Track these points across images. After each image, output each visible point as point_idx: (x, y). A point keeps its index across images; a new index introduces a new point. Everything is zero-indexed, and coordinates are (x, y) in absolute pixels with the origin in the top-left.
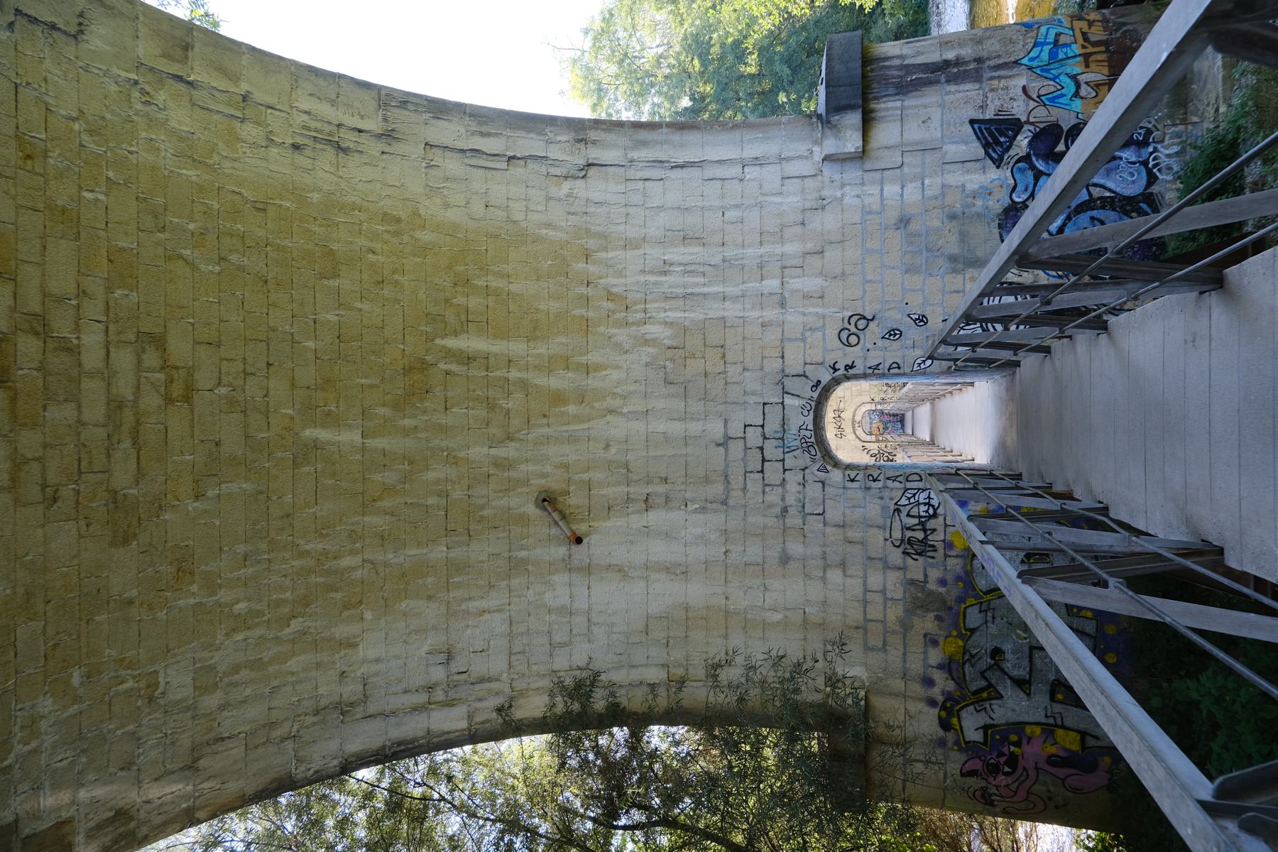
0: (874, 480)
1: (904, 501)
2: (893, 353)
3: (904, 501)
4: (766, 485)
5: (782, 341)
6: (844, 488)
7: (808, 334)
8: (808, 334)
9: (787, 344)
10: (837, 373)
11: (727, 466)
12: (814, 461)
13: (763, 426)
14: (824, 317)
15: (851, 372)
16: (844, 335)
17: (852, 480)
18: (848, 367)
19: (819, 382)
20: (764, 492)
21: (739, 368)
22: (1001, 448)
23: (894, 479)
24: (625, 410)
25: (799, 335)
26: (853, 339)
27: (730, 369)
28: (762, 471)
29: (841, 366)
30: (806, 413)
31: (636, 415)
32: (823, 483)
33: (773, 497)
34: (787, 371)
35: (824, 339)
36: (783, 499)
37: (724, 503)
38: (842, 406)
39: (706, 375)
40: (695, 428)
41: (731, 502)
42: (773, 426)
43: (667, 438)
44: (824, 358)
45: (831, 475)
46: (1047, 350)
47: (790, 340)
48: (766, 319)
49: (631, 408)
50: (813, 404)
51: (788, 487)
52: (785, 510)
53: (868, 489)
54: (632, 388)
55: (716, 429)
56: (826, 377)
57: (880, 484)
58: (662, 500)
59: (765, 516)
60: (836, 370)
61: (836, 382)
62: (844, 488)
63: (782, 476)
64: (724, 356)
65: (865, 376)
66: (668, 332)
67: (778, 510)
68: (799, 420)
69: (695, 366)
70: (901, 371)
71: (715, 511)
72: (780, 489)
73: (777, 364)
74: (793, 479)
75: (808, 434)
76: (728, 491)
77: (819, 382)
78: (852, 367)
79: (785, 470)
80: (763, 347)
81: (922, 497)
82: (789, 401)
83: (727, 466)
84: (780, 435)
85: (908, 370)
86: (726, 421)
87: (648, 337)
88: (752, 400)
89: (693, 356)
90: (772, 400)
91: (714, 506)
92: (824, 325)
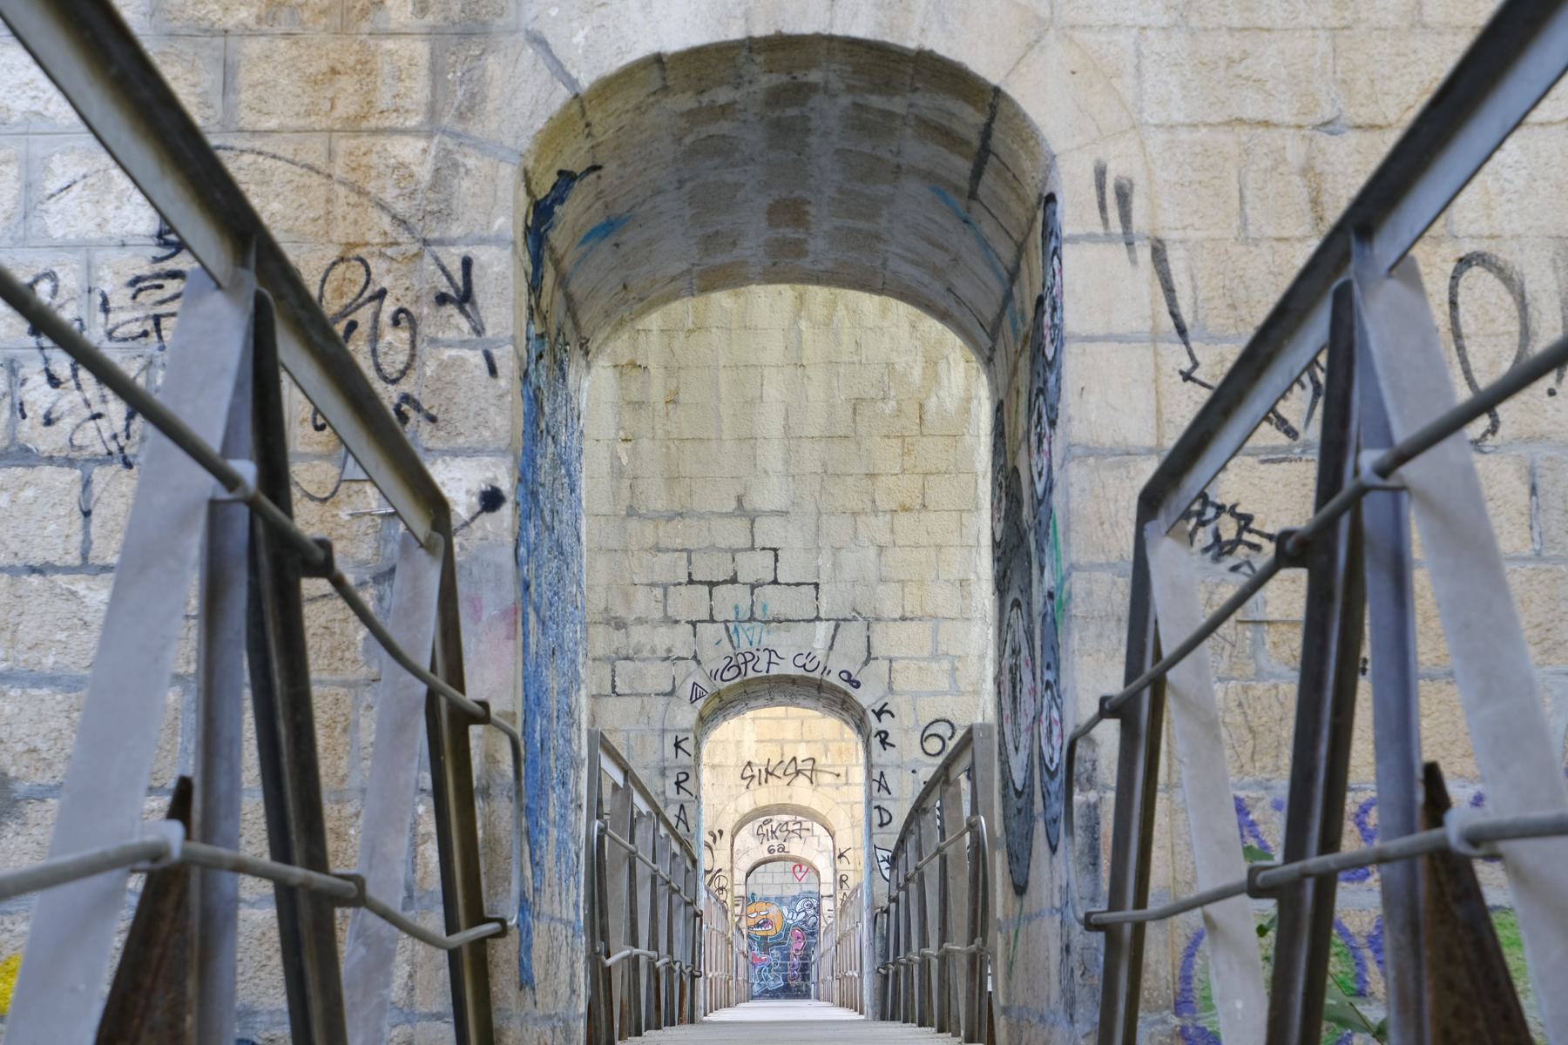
0: (678, 784)
4: (665, 588)
5: (934, 617)
6: (664, 731)
7: (946, 665)
8: (946, 665)
9: (927, 626)
10: (872, 717)
11: (701, 516)
12: (713, 676)
13: (775, 582)
14: (976, 693)
15: (875, 742)
16: (943, 729)
17: (677, 745)
18: (884, 738)
19: (858, 685)
20: (652, 585)
21: (884, 538)
24: (803, 325)
25: (943, 647)
27: (882, 521)
28: (691, 582)
29: (886, 723)
30: (800, 661)
31: (795, 345)
32: (671, 693)
33: (644, 603)
34: (877, 628)
35: (935, 694)
36: (640, 621)
37: (632, 512)
38: (826, 778)
39: (871, 476)
40: (772, 455)
41: (633, 525)
42: (775, 601)
43: (752, 403)
44: (903, 693)
45: (687, 707)
47: (936, 631)
48: (973, 588)
49: (807, 334)
50: (816, 675)
51: (663, 630)
52: (620, 624)
53: (663, 773)
54: (846, 339)
55: (768, 495)
56: (866, 697)
58: (635, 395)
59: (608, 588)
60: (879, 714)
61: (860, 725)
62: (664, 731)
63: (683, 618)
64: (906, 509)
65: (869, 767)
66: (951, 405)
67: (619, 611)
68: (787, 652)
69: (886, 456)
70: (876, 829)
71: (615, 495)
72: (658, 615)
73: (890, 609)
74: (679, 640)
75: (762, 666)
76: (654, 517)
77: (858, 685)
78: (883, 742)
79: (693, 624)
80: (921, 582)
82: (822, 631)
83: (701, 516)
84: (758, 614)
85: (877, 840)
86: (783, 513)
87: (942, 366)
88: (825, 562)
89: (906, 452)
90: (823, 599)
91: (626, 493)
92: (963, 694)
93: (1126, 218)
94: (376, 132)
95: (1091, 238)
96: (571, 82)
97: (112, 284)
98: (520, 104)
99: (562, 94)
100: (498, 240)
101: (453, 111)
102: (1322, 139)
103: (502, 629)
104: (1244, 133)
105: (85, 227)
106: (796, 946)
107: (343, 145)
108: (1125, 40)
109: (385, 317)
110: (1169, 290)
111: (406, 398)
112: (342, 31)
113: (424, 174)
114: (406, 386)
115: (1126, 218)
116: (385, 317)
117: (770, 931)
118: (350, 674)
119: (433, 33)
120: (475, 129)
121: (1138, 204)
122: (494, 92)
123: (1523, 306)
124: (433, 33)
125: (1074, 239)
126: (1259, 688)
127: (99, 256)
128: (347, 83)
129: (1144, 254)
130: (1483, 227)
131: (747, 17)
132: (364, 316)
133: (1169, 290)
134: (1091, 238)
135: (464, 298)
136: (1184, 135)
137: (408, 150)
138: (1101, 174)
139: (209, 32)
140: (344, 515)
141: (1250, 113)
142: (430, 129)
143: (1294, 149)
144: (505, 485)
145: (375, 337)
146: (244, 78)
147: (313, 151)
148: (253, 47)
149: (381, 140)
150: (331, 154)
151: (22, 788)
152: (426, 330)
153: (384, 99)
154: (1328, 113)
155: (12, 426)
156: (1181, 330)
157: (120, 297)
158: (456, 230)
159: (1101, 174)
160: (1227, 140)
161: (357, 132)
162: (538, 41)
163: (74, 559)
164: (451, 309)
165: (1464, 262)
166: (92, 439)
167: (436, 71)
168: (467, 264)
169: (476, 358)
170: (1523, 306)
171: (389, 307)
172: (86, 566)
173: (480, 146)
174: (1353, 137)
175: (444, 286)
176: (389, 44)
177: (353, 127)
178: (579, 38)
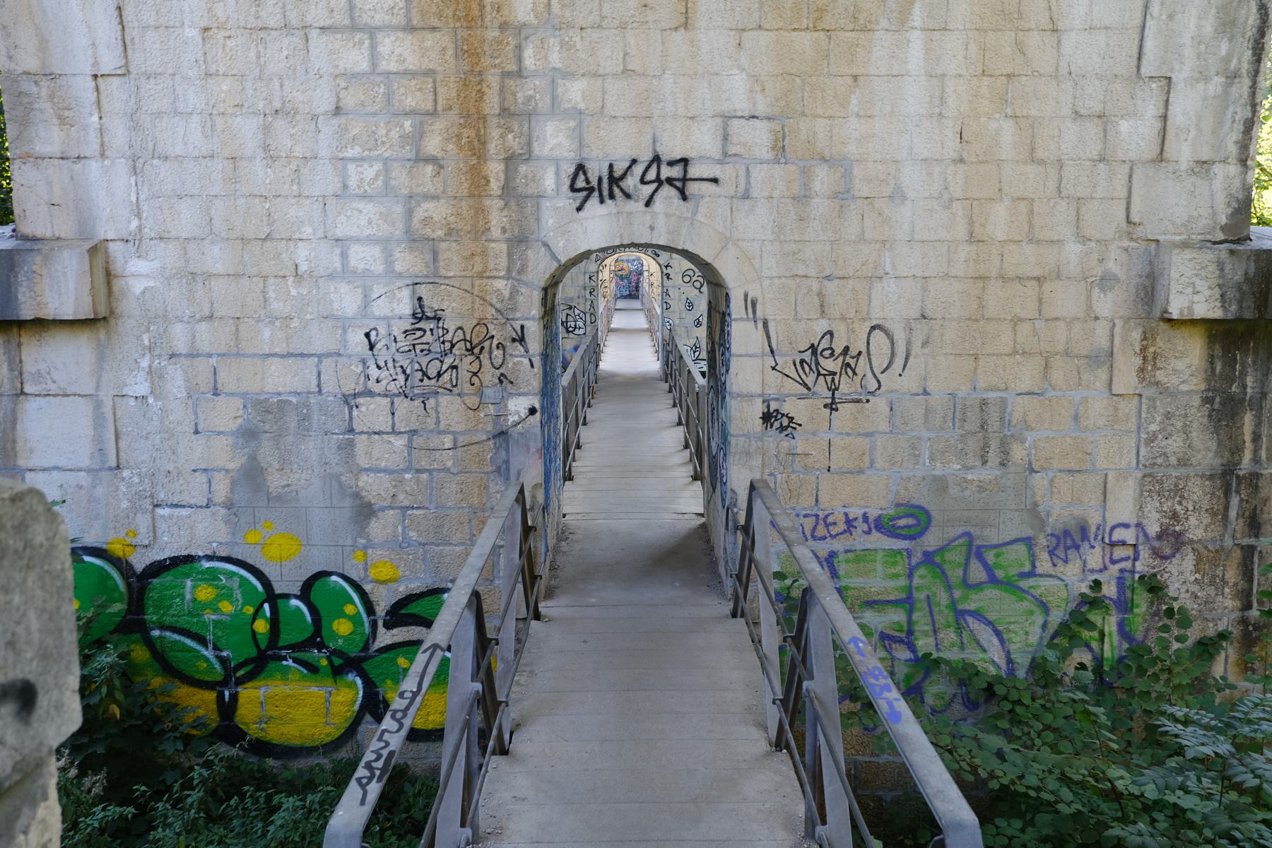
1: (577, 312)
2: (677, 305)
3: (577, 312)
18: (668, 276)
22: (611, 376)
23: (592, 306)
26: (687, 279)
29: (669, 270)
46: (670, 391)
57: (588, 296)
81: (580, 323)
93: (754, 312)
94: (489, 277)
95: (741, 319)
96: (558, 261)
97: (397, 332)
98: (540, 268)
99: (555, 265)
100: (533, 319)
101: (516, 271)
102: (826, 282)
103: (537, 456)
104: (798, 280)
105: (386, 312)
106: (634, 279)
107: (477, 282)
108: (757, 245)
109: (494, 346)
110: (768, 337)
111: (502, 375)
112: (476, 239)
113: (506, 293)
114: (502, 371)
115: (754, 312)
116: (494, 346)
117: (623, 273)
118: (485, 470)
119: (508, 241)
120: (524, 278)
121: (759, 307)
122: (530, 264)
123: (893, 344)
124: (508, 241)
125: (736, 320)
126: (793, 476)
127: (392, 322)
128: (478, 259)
129: (760, 325)
130: (880, 315)
131: (621, 236)
132: (486, 344)
133: (768, 337)
134: (741, 319)
135: (522, 340)
136: (776, 281)
137: (500, 284)
138: (746, 296)
139: (428, 239)
140: (482, 415)
141: (800, 273)
142: (508, 277)
143: (815, 286)
144: (537, 406)
145: (490, 352)
146: (441, 257)
147: (467, 284)
148: (444, 245)
149: (490, 281)
150: (473, 286)
151: (376, 507)
152: (509, 351)
153: (491, 266)
154: (828, 272)
155: (365, 383)
156: (772, 352)
157: (400, 337)
158: (518, 315)
159: (746, 296)
160: (790, 281)
161: (482, 277)
162: (546, 245)
163: (389, 429)
164: (517, 344)
165: (873, 328)
166: (393, 388)
167: (510, 255)
168: (522, 327)
169: (526, 361)
170: (893, 344)
171: (495, 342)
172: (394, 432)
173: (526, 284)
174: (836, 282)
175: (514, 336)
176: (493, 245)
177: (480, 276)
178: (561, 244)
